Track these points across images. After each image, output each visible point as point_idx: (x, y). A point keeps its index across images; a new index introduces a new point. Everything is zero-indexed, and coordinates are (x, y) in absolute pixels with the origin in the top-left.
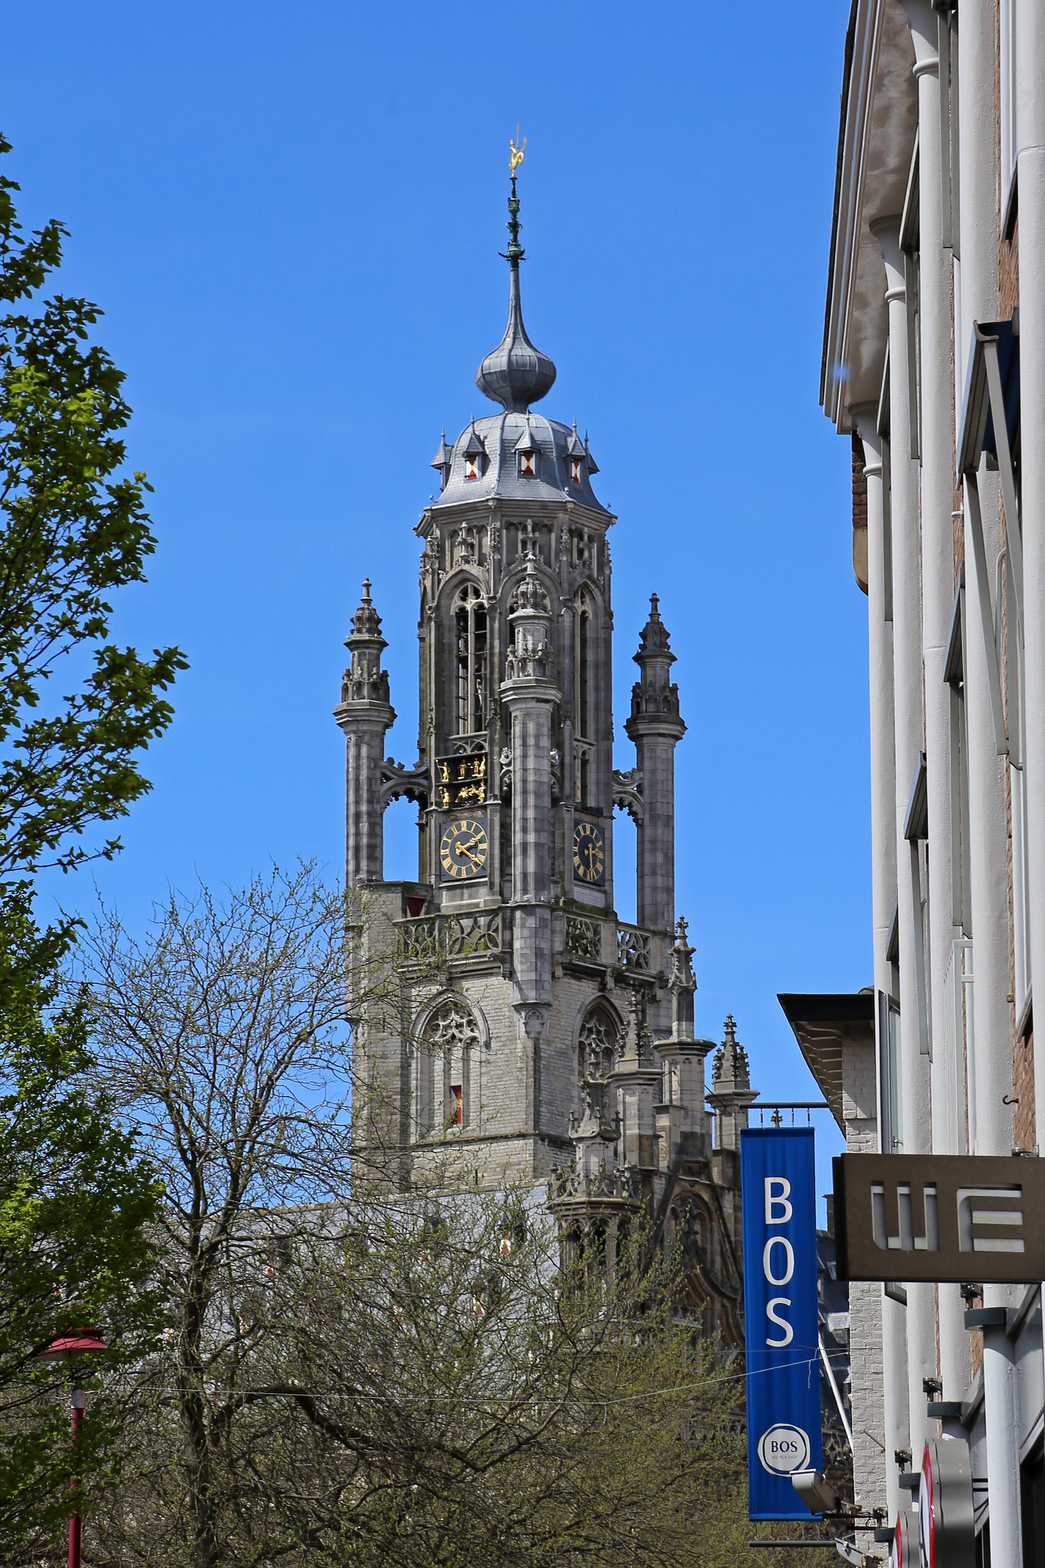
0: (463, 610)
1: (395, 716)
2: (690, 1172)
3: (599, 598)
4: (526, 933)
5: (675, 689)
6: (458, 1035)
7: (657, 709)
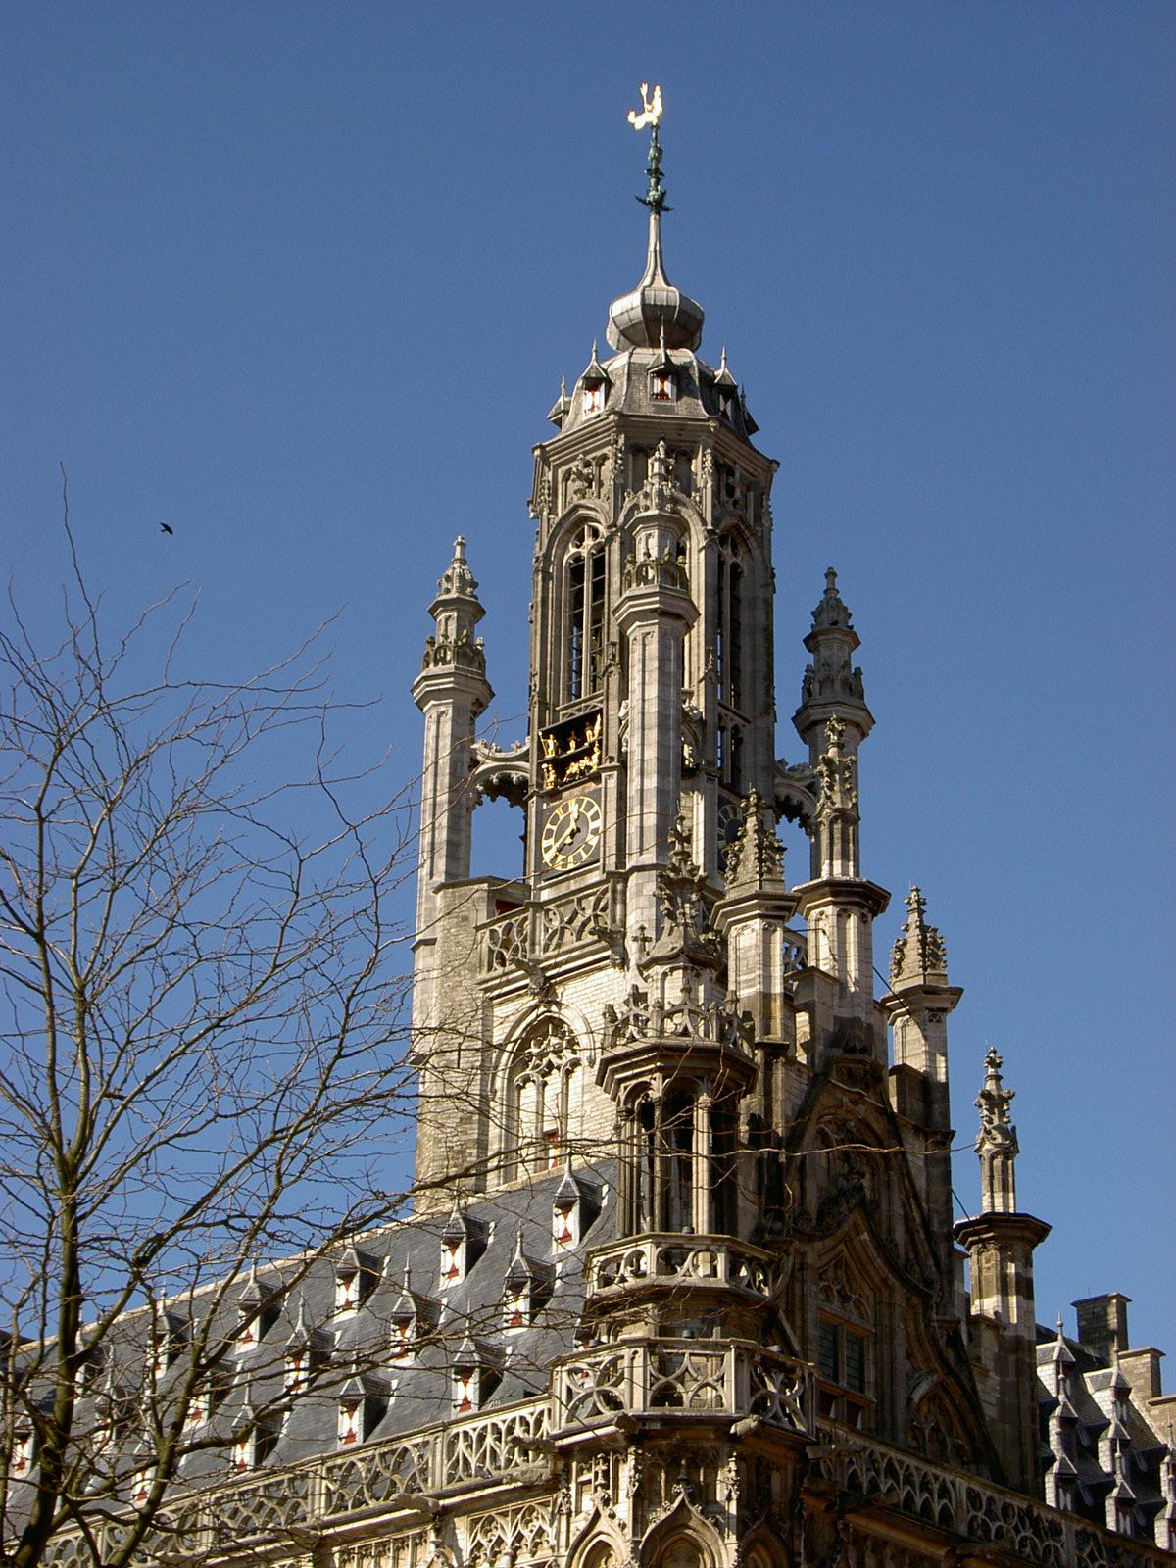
0: (578, 558)
1: (493, 695)
2: (851, 1078)
3: (756, 553)
4: (643, 902)
5: (858, 672)
6: (555, 1061)
7: (836, 693)
